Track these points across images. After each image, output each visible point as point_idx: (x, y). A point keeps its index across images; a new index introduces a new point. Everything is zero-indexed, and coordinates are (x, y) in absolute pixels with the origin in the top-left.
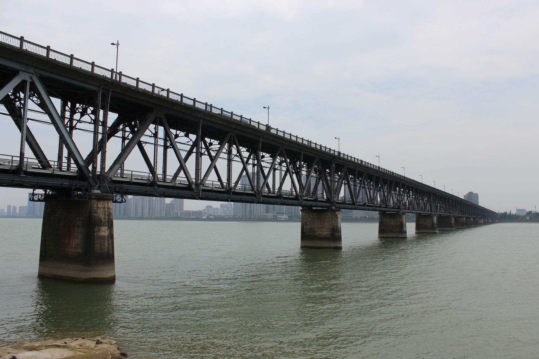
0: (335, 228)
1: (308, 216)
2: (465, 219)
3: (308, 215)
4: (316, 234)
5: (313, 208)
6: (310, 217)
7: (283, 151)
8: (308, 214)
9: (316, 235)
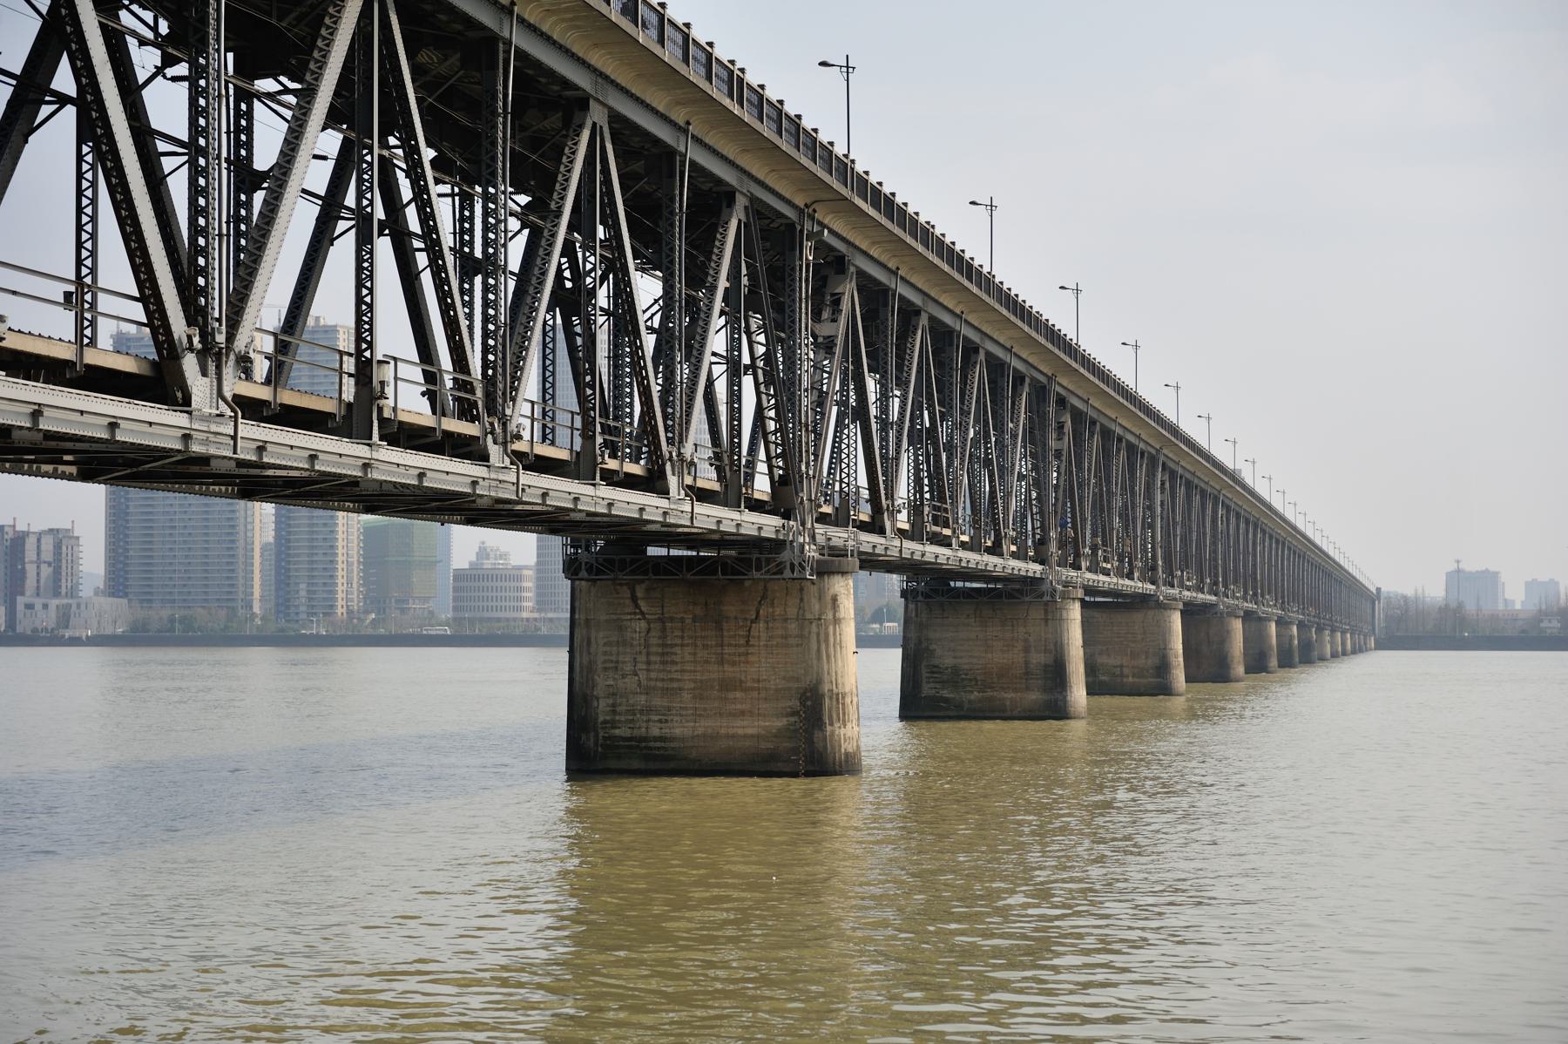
0: (826, 688)
1: (631, 609)
2: (1295, 629)
3: (628, 602)
4: (688, 732)
5: (653, 551)
6: (642, 613)
7: (601, 127)
8: (626, 592)
9: (683, 740)
